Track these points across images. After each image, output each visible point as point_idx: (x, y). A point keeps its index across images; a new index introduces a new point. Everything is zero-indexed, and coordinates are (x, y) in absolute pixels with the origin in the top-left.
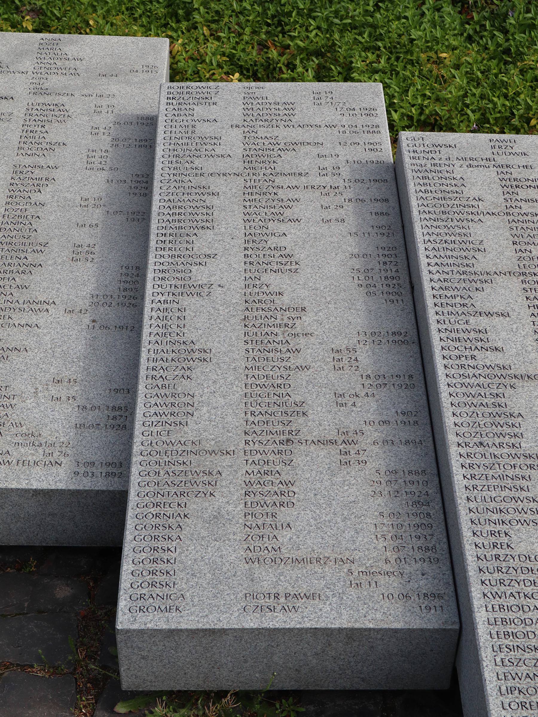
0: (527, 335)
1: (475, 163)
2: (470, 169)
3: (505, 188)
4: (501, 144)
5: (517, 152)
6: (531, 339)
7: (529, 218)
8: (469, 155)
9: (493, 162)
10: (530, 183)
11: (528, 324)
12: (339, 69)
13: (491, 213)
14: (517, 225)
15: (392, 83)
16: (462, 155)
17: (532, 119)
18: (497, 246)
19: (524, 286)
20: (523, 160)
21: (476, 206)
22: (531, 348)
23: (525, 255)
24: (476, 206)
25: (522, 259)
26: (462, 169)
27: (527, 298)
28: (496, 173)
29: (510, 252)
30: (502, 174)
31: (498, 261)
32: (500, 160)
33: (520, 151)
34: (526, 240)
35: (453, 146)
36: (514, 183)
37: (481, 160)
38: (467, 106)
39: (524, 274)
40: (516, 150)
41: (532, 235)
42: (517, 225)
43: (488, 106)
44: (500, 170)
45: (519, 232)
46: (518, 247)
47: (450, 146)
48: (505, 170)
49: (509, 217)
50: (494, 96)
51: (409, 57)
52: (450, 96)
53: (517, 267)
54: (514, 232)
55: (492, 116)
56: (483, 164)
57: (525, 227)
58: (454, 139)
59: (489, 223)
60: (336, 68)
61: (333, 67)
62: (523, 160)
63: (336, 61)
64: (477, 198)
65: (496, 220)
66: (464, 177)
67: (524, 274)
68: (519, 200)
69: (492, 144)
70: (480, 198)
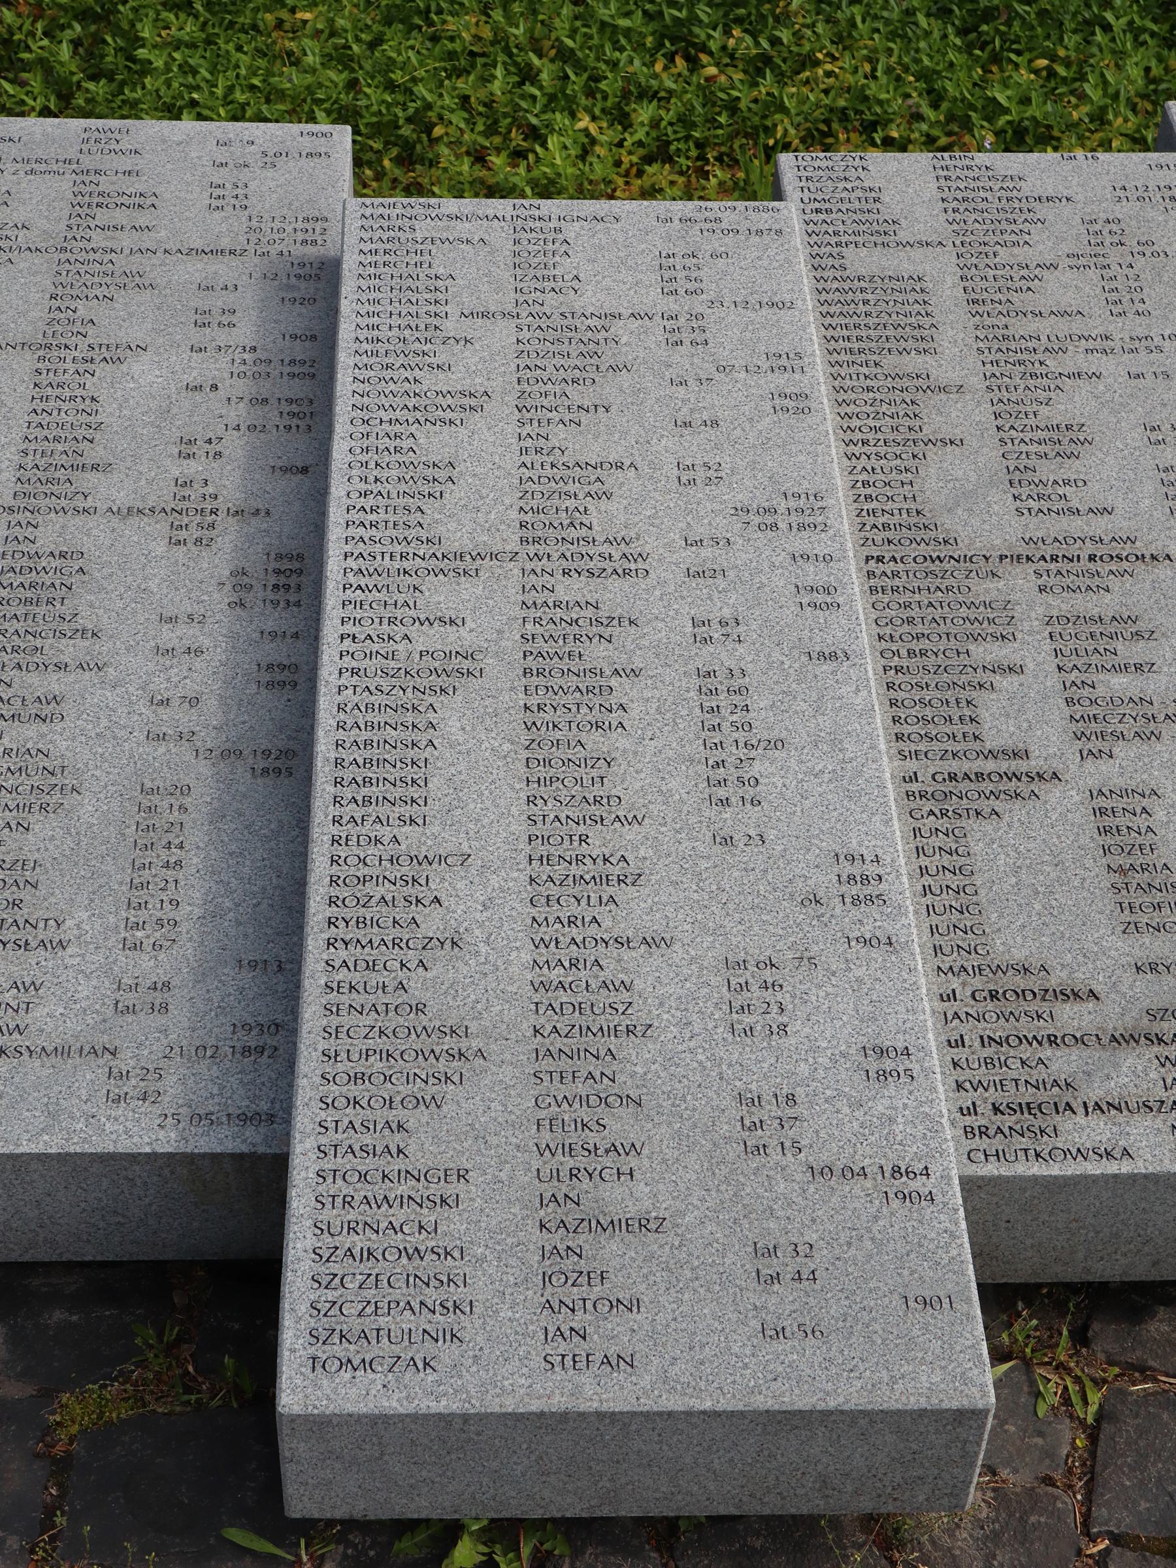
0: (9, 443)
1: (43, 167)
2: (29, 177)
3: (78, 207)
4: (102, 136)
5: (123, 148)
6: (13, 449)
7: (97, 256)
8: (40, 154)
9: (74, 166)
10: (125, 200)
11: (20, 426)
12: (119, 41)
13: (33, 249)
14: (71, 267)
15: (201, 66)
16: (25, 155)
17: (436, 125)
18: (21, 302)
19: (40, 365)
20: (127, 163)
21: (13, 238)
22: (7, 463)
23: (62, 316)
24: (13, 238)
25: (55, 322)
26: (15, 177)
27: (36, 385)
28: (71, 184)
29: (38, 313)
30: (82, 186)
31: (12, 325)
32: (87, 162)
33: (130, 147)
34: (74, 293)
35: (16, 139)
36: (96, 200)
37: (54, 162)
38: (318, 102)
39: (48, 347)
40: (125, 145)
41: (89, 284)
42: (71, 267)
43: (359, 103)
44: (79, 179)
45: (69, 280)
46: (55, 304)
47: (10, 140)
48: (87, 179)
49: (62, 256)
50: (369, 86)
51: (241, 20)
52: (288, 85)
53: (41, 336)
54: (63, 279)
55: (365, 121)
56: (55, 169)
57: (82, 272)
58: (21, 128)
59: (22, 265)
60: (115, 42)
61: (109, 39)
62: (127, 163)
63: (117, 31)
64: (20, 225)
65: (37, 259)
66: (13, 191)
67: (48, 347)
68: (93, 227)
69: (86, 136)
70: (26, 224)
